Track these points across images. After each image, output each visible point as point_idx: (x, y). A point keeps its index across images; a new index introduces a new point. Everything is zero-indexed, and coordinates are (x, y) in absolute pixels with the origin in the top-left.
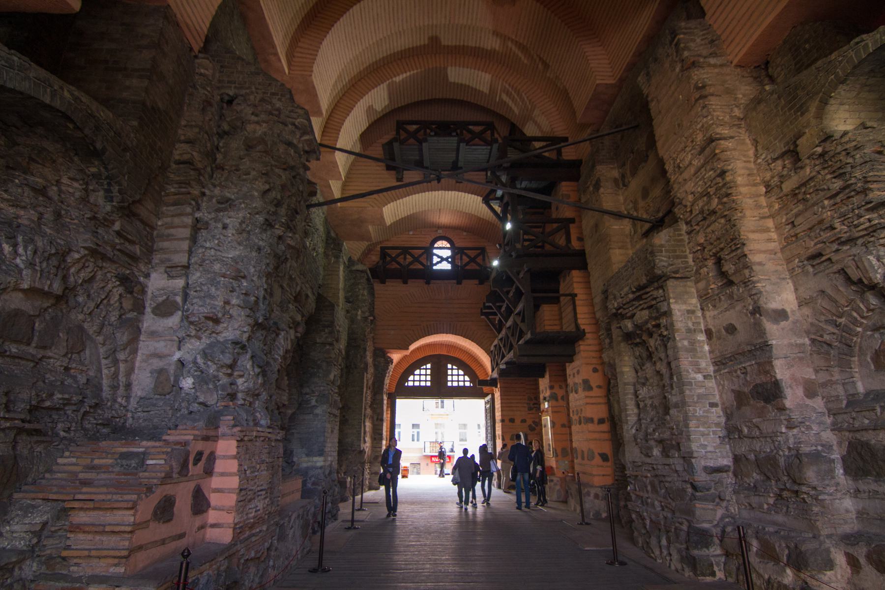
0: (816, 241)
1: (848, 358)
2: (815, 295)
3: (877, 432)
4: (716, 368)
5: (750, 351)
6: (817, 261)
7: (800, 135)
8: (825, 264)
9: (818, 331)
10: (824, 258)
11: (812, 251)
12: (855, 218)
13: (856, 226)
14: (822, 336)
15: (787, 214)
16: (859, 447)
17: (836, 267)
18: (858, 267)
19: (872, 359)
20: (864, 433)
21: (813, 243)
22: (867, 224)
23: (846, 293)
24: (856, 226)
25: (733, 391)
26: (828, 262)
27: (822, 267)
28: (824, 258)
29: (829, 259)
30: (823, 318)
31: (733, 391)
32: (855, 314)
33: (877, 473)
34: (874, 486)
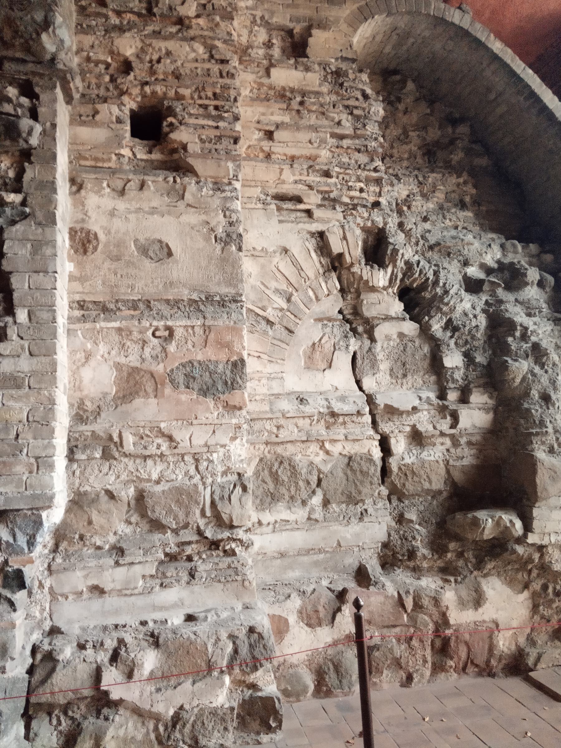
0: (297, 178)
1: (284, 346)
2: (271, 250)
3: (308, 444)
4: (78, 313)
5: (192, 302)
6: (288, 205)
7: (323, 25)
8: (299, 214)
9: (261, 300)
10: (302, 207)
11: (289, 188)
12: (354, 178)
13: (350, 188)
14: (264, 309)
15: (263, 114)
16: (276, 465)
17: (316, 227)
18: (345, 238)
19: (305, 352)
20: (289, 446)
21: (292, 179)
22: (357, 194)
23: (313, 264)
24: (350, 188)
25: (118, 366)
26: (303, 215)
27: (293, 215)
28: (302, 207)
29: (309, 213)
30: (273, 285)
31: (118, 366)
32: (311, 293)
33: (292, 498)
34: (285, 515)
